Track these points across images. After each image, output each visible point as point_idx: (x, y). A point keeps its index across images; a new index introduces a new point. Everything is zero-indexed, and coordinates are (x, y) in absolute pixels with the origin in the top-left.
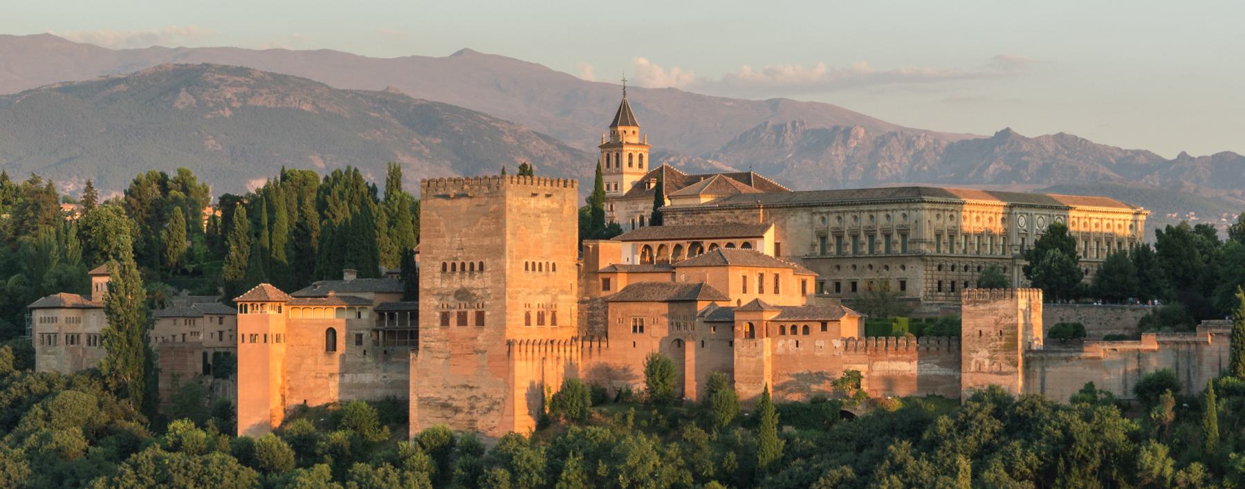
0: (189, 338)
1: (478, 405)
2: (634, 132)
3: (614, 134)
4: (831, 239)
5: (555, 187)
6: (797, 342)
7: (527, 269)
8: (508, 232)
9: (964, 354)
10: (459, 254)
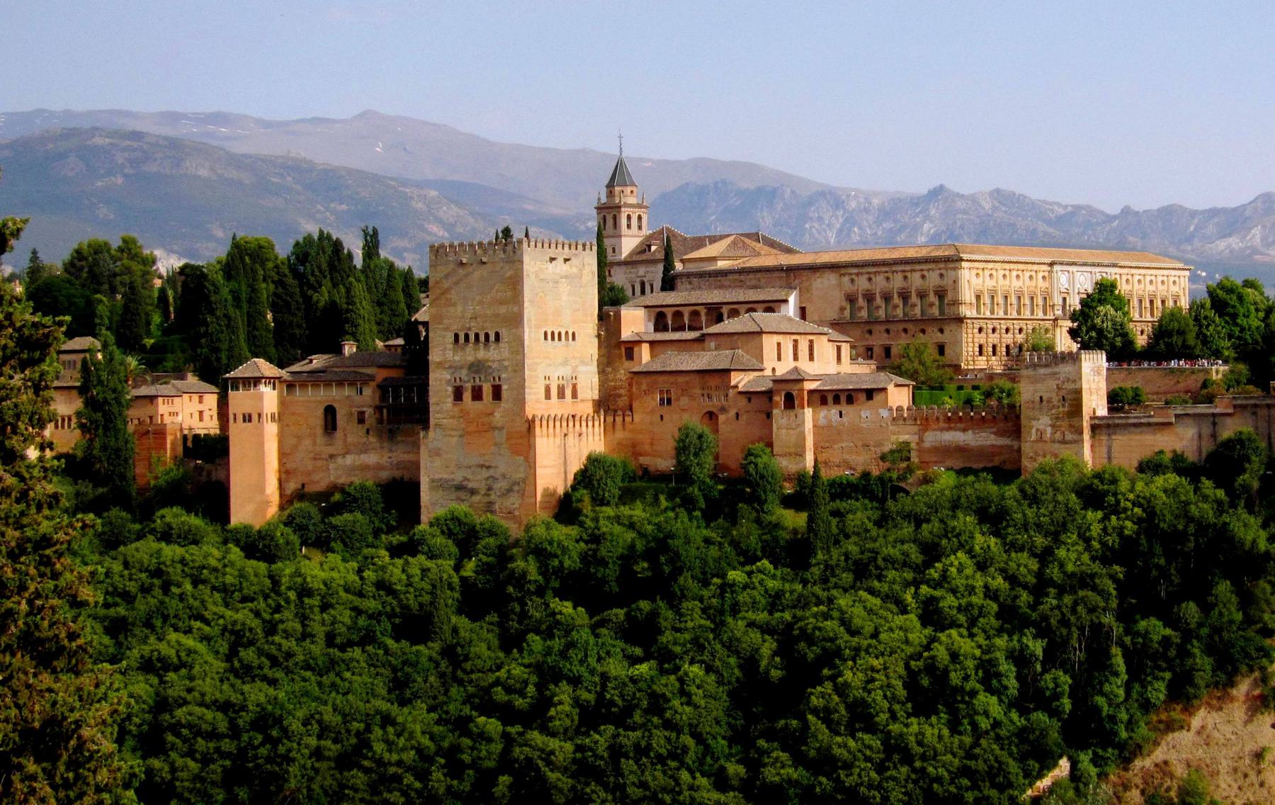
0: (167, 420)
1: (497, 486)
2: (632, 192)
3: (611, 194)
4: (861, 302)
5: (573, 250)
6: (841, 413)
7: (546, 338)
8: (526, 299)
9: (1024, 421)
10: (472, 324)
